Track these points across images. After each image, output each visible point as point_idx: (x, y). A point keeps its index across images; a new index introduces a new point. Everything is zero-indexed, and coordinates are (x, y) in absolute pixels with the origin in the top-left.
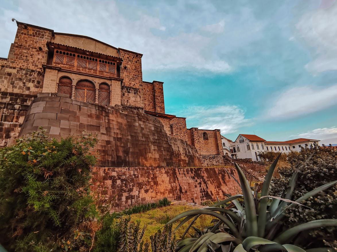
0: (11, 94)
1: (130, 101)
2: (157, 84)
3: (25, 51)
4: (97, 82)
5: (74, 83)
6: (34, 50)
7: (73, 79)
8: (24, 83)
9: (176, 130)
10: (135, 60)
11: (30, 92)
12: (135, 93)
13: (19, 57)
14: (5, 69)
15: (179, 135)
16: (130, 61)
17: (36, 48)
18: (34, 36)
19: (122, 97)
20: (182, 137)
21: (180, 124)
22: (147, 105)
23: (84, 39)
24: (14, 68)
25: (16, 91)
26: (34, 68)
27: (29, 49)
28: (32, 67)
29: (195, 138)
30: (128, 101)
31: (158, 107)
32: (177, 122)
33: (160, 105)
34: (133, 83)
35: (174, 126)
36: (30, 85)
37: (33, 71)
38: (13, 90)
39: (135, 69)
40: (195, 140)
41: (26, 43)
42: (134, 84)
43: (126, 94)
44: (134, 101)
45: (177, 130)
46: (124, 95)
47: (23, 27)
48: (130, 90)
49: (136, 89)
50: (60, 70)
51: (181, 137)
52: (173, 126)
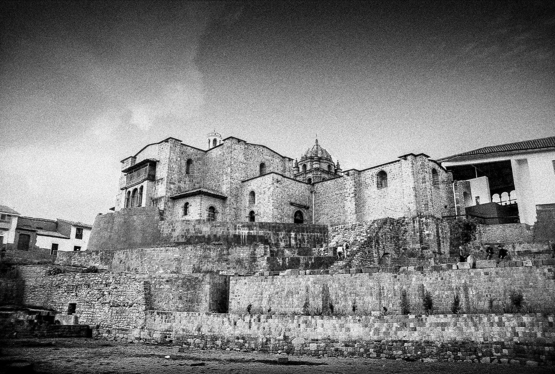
21: (263, 186)
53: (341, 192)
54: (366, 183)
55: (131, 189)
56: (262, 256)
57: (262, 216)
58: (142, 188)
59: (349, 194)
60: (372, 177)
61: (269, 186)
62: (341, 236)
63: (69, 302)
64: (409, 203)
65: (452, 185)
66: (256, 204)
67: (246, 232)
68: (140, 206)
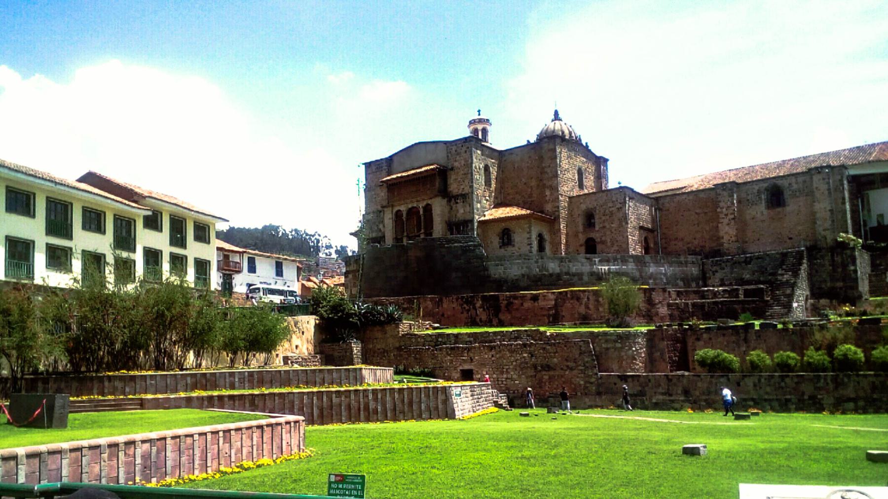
1: (459, 215)
2: (546, 142)
5: (404, 215)
9: (601, 218)
10: (464, 149)
12: (463, 202)
15: (608, 227)
16: (458, 154)
18: (376, 172)
19: (449, 212)
20: (615, 230)
21: (610, 205)
22: (534, 189)
29: (721, 212)
30: (456, 215)
31: (548, 188)
32: (604, 200)
33: (550, 183)
34: (462, 187)
35: (597, 211)
36: (381, 226)
37: (380, 212)
39: (464, 165)
40: (722, 216)
42: (463, 189)
43: (454, 206)
44: (463, 213)
45: (604, 218)
46: (451, 209)
47: (368, 165)
48: (458, 199)
49: (464, 195)
51: (613, 230)
52: (595, 211)
53: (706, 211)
54: (748, 200)
55: (403, 208)
56: (660, 302)
57: (609, 244)
58: (428, 209)
59: (726, 215)
60: (758, 193)
61: (619, 206)
62: (727, 270)
63: (461, 368)
64: (824, 230)
65: (858, 202)
66: (597, 228)
67: (607, 268)
68: (429, 233)
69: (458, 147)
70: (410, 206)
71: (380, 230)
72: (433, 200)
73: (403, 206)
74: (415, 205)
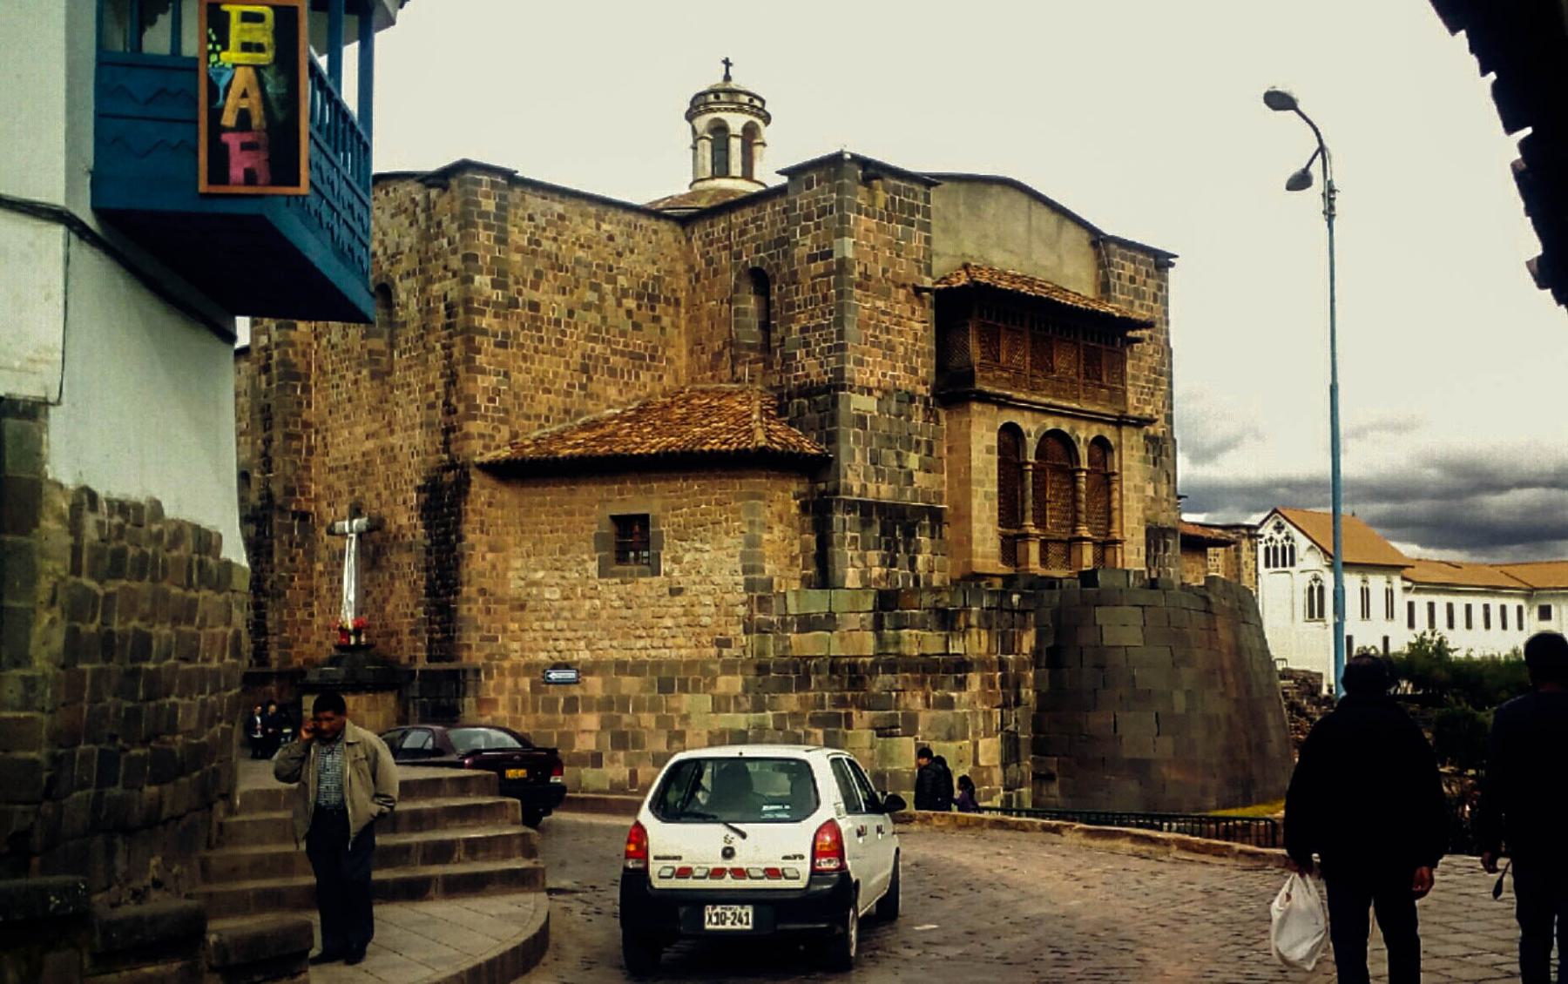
0: (882, 508)
3: (881, 304)
4: (1082, 436)
6: (902, 294)
7: (1029, 435)
8: (899, 455)
11: (915, 491)
13: (872, 336)
14: (849, 397)
17: (904, 286)
23: (996, 189)
24: (870, 392)
25: (884, 492)
26: (911, 381)
27: (886, 295)
28: (905, 383)
38: (878, 488)
41: (876, 261)
50: (1003, 403)
69: (1136, 271)
70: (1050, 423)
71: (910, 475)
72: (1125, 431)
73: (1027, 414)
74: (1065, 426)
